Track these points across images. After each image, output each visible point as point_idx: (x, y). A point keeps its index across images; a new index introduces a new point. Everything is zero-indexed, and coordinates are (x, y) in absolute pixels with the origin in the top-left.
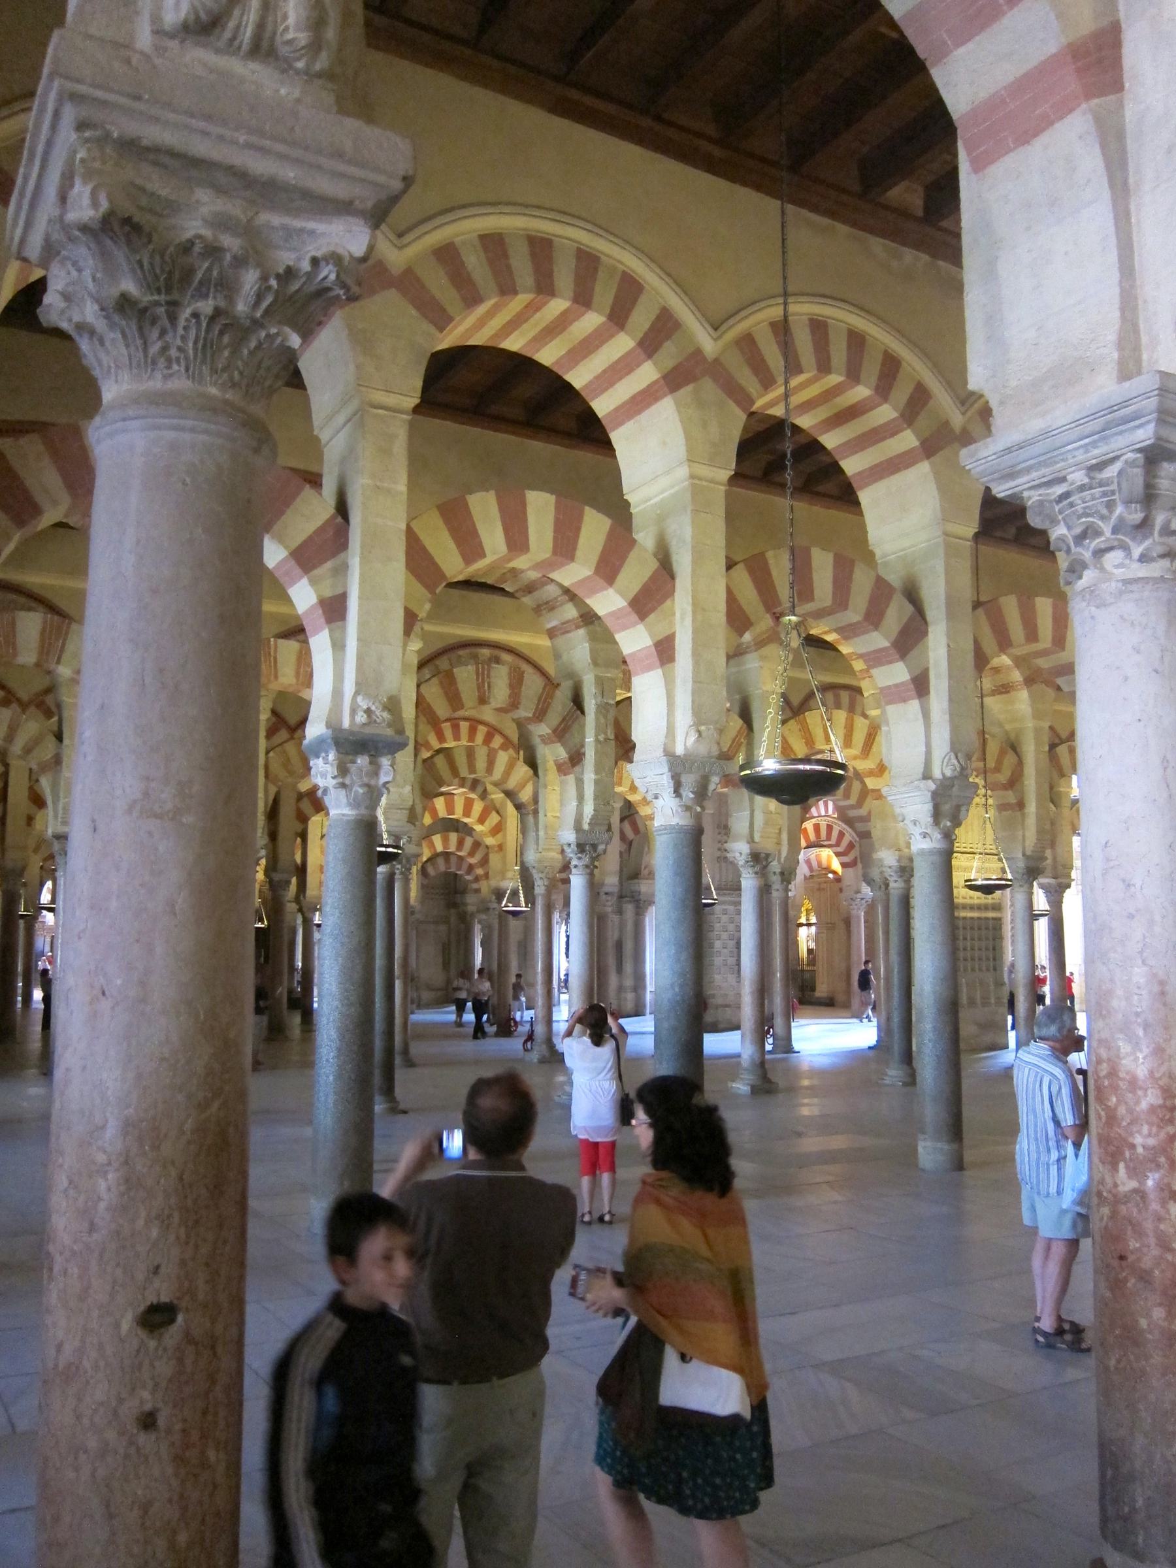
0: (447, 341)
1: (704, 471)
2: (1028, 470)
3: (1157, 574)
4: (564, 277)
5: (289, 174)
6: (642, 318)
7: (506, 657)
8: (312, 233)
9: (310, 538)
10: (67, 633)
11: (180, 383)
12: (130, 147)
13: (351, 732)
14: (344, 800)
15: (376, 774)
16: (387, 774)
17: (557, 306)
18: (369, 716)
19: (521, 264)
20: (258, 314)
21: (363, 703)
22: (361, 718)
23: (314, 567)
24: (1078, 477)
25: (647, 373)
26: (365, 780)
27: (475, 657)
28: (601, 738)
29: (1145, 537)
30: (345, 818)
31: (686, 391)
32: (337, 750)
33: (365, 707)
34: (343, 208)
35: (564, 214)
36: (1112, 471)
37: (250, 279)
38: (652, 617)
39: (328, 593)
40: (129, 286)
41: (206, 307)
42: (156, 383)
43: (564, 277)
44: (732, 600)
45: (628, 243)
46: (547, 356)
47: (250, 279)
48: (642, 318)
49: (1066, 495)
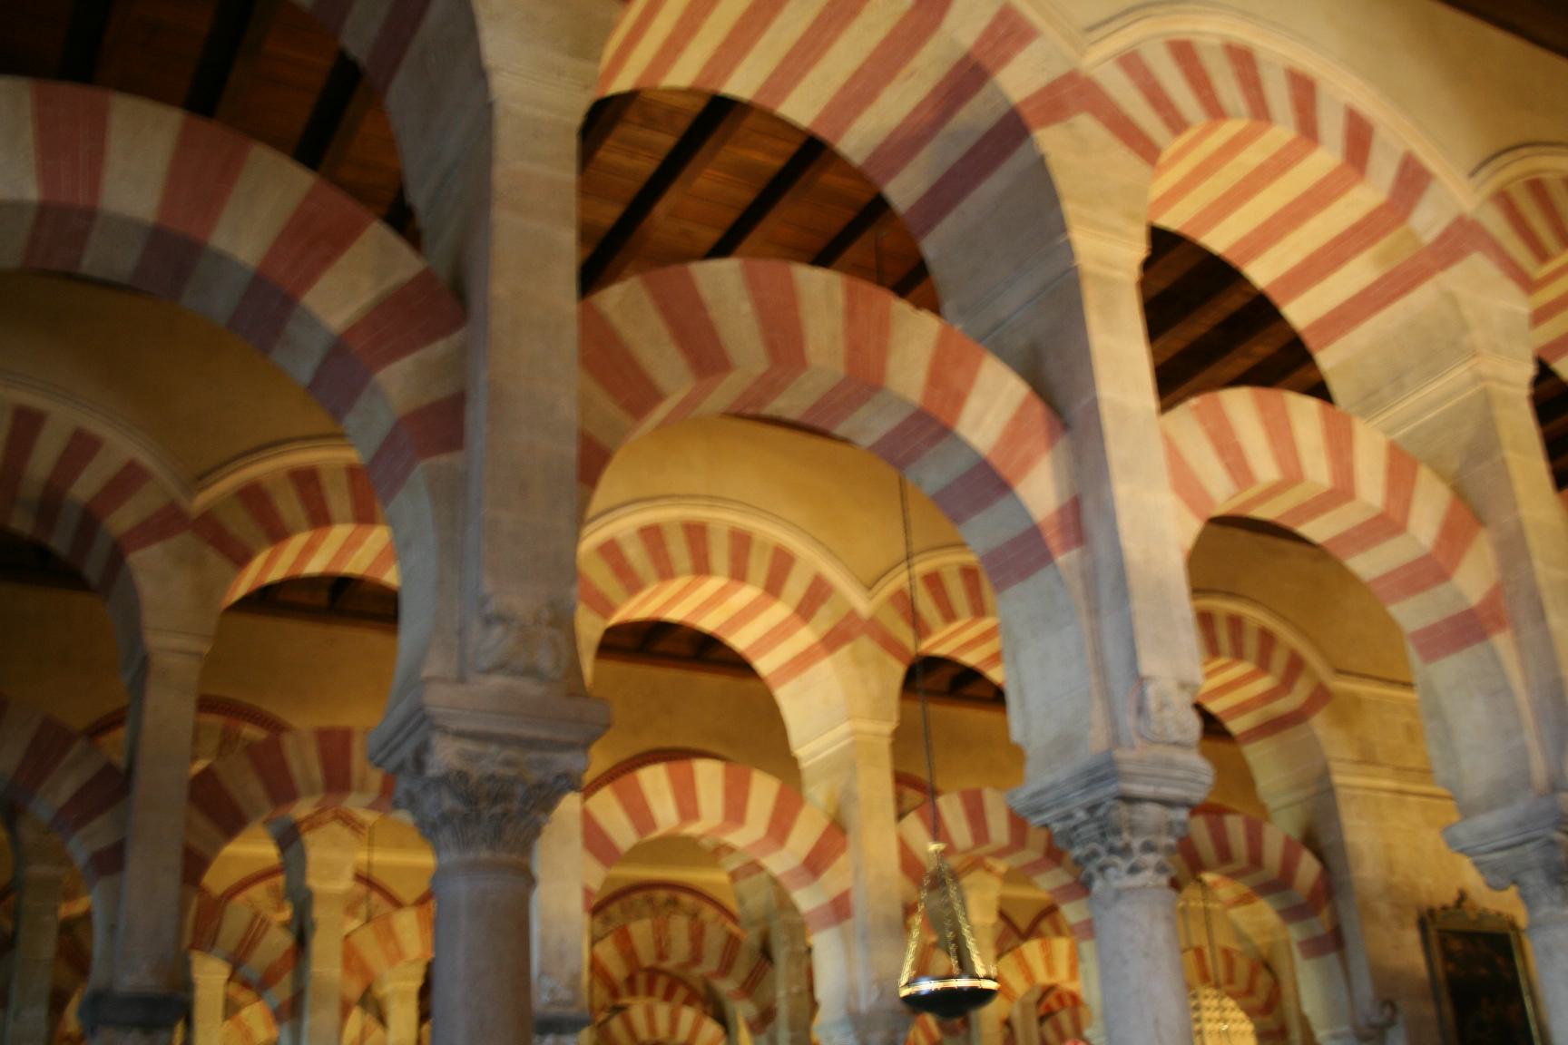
0: (616, 619)
1: (867, 726)
2: (1047, 810)
4: (720, 555)
6: (796, 587)
7: (686, 899)
11: (485, 854)
12: (460, 735)
17: (713, 584)
19: (678, 549)
20: (528, 808)
24: (1081, 815)
25: (805, 637)
27: (650, 901)
28: (795, 989)
31: (844, 652)
35: (713, 500)
36: (1101, 812)
37: (519, 790)
38: (826, 876)
40: (460, 806)
41: (498, 809)
42: (471, 855)
43: (720, 555)
44: (905, 849)
45: (776, 518)
46: (708, 624)
47: (519, 790)
48: (796, 587)
49: (1075, 828)
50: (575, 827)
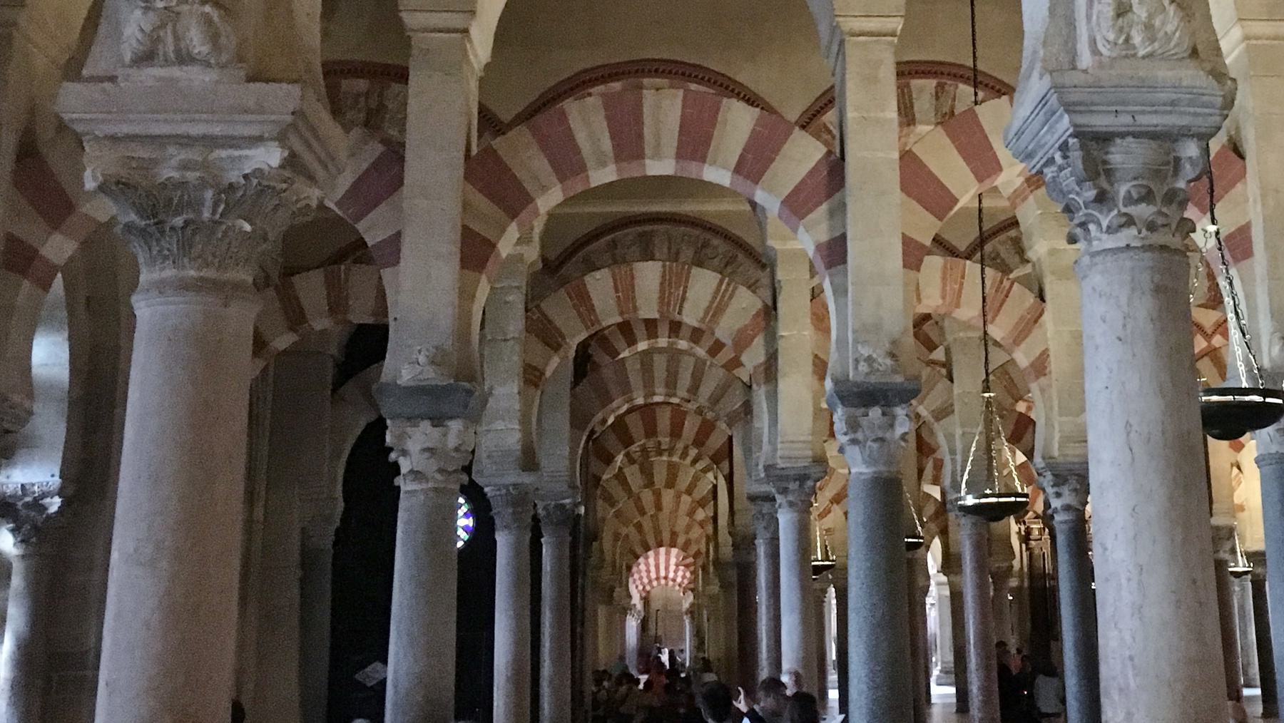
3: (1123, 244)
5: (217, 130)
8: (247, 157)
9: (803, 182)
10: (687, 280)
13: (856, 384)
14: (859, 457)
15: (892, 426)
16: (901, 425)
18: (870, 366)
20: (218, 216)
21: (865, 351)
22: (863, 367)
23: (810, 211)
24: (1058, 157)
26: (880, 434)
29: (1110, 210)
30: (863, 477)
32: (843, 404)
33: (866, 355)
34: (257, 140)
39: (824, 237)
50: (893, 177)
